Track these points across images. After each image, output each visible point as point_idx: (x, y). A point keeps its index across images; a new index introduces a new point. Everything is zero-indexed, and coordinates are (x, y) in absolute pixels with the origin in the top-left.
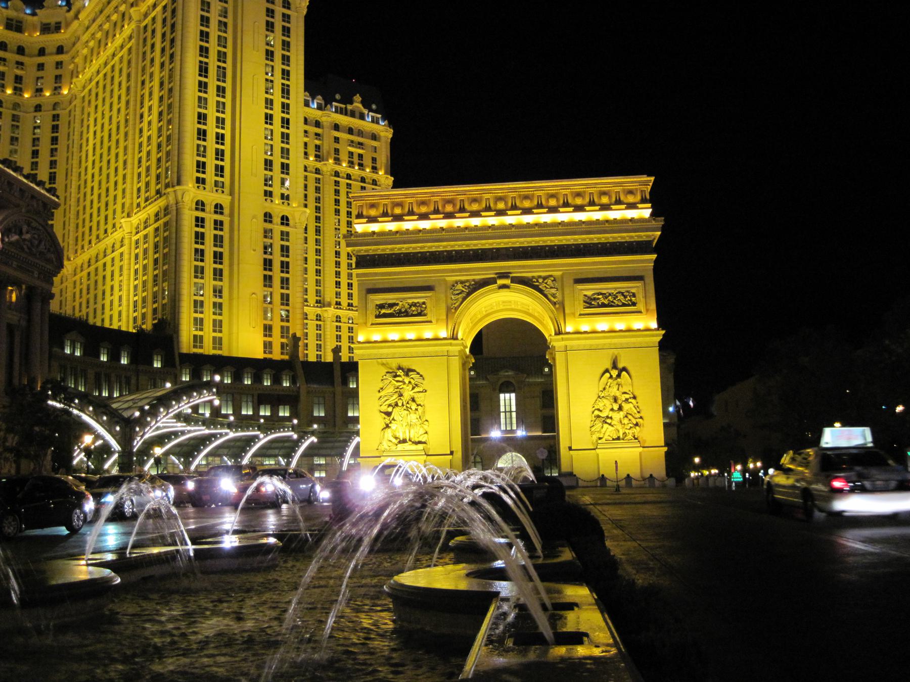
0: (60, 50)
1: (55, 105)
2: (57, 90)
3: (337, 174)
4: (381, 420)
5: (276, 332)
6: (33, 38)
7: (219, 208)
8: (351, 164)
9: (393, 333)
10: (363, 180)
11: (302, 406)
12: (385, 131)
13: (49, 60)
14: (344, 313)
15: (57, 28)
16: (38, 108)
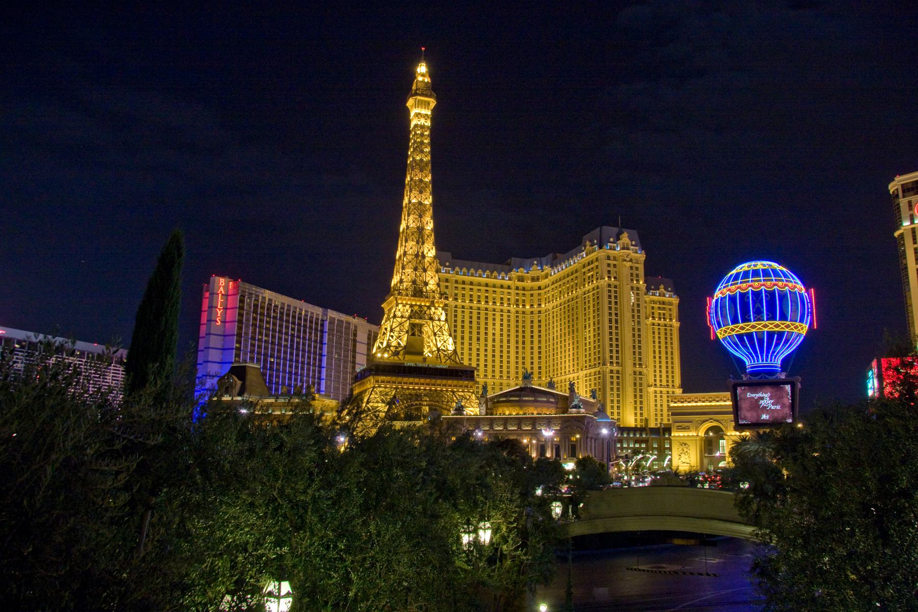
0: (540, 288)
1: (540, 312)
2: (540, 305)
3: (653, 324)
4: (678, 457)
5: (638, 415)
6: (528, 284)
7: (618, 372)
8: (660, 319)
9: (681, 434)
10: (665, 325)
11: (649, 443)
12: (675, 301)
13: (536, 292)
14: (658, 389)
15: (538, 279)
16: (532, 313)
